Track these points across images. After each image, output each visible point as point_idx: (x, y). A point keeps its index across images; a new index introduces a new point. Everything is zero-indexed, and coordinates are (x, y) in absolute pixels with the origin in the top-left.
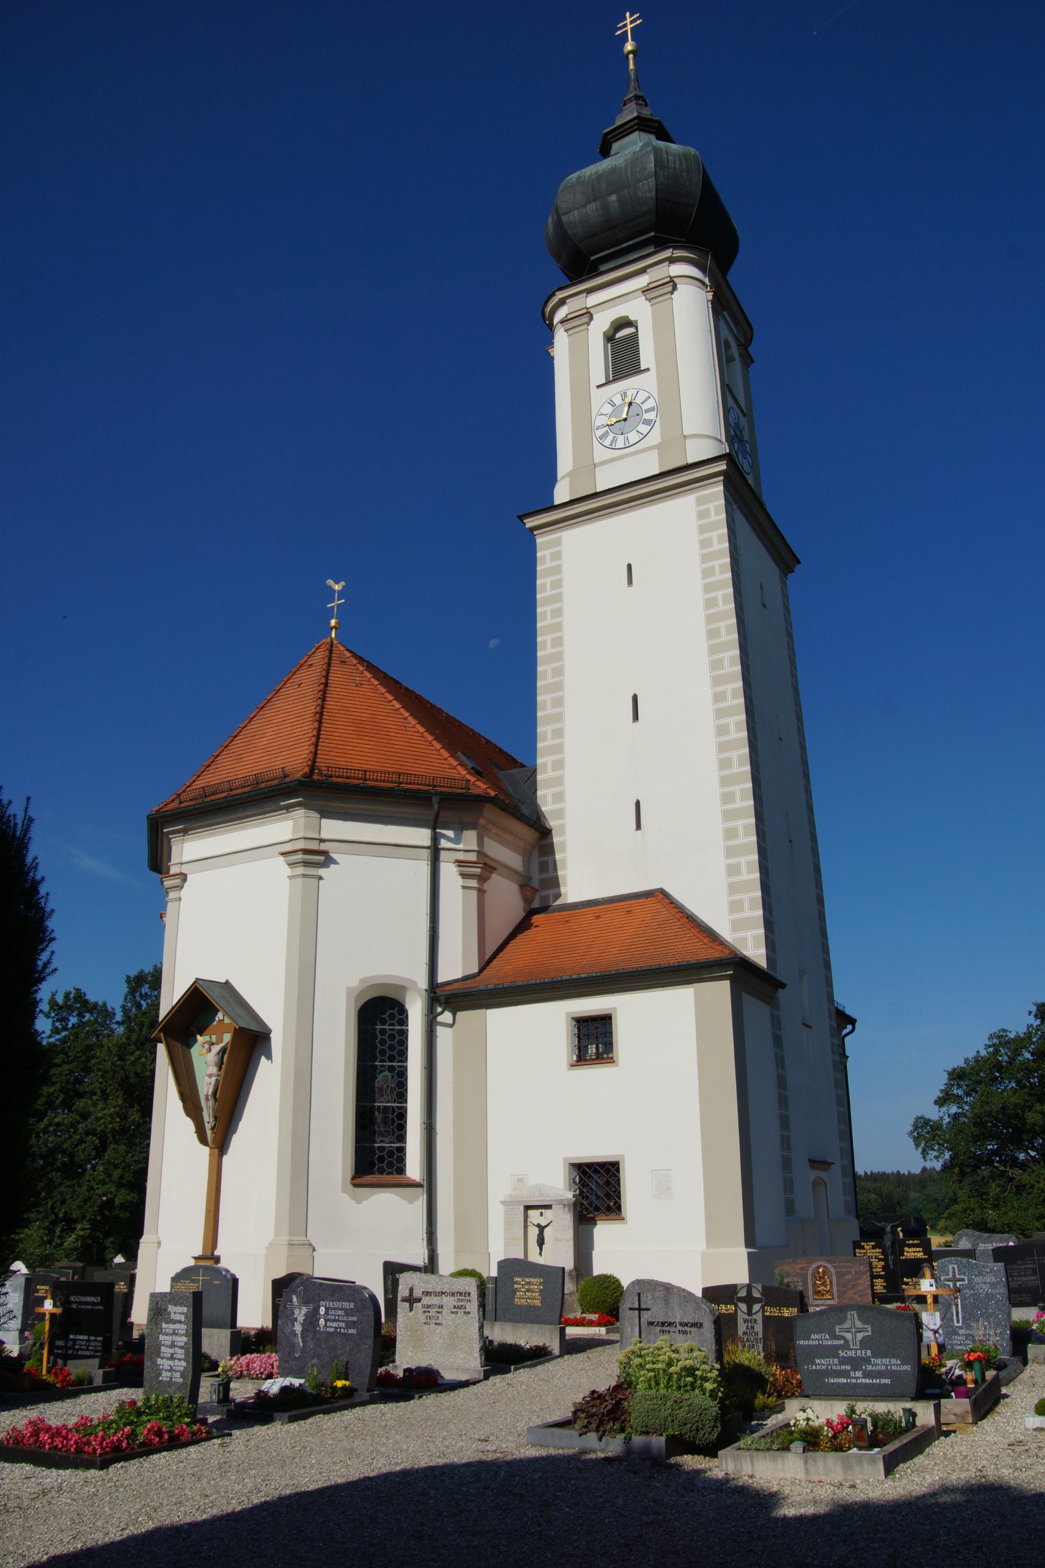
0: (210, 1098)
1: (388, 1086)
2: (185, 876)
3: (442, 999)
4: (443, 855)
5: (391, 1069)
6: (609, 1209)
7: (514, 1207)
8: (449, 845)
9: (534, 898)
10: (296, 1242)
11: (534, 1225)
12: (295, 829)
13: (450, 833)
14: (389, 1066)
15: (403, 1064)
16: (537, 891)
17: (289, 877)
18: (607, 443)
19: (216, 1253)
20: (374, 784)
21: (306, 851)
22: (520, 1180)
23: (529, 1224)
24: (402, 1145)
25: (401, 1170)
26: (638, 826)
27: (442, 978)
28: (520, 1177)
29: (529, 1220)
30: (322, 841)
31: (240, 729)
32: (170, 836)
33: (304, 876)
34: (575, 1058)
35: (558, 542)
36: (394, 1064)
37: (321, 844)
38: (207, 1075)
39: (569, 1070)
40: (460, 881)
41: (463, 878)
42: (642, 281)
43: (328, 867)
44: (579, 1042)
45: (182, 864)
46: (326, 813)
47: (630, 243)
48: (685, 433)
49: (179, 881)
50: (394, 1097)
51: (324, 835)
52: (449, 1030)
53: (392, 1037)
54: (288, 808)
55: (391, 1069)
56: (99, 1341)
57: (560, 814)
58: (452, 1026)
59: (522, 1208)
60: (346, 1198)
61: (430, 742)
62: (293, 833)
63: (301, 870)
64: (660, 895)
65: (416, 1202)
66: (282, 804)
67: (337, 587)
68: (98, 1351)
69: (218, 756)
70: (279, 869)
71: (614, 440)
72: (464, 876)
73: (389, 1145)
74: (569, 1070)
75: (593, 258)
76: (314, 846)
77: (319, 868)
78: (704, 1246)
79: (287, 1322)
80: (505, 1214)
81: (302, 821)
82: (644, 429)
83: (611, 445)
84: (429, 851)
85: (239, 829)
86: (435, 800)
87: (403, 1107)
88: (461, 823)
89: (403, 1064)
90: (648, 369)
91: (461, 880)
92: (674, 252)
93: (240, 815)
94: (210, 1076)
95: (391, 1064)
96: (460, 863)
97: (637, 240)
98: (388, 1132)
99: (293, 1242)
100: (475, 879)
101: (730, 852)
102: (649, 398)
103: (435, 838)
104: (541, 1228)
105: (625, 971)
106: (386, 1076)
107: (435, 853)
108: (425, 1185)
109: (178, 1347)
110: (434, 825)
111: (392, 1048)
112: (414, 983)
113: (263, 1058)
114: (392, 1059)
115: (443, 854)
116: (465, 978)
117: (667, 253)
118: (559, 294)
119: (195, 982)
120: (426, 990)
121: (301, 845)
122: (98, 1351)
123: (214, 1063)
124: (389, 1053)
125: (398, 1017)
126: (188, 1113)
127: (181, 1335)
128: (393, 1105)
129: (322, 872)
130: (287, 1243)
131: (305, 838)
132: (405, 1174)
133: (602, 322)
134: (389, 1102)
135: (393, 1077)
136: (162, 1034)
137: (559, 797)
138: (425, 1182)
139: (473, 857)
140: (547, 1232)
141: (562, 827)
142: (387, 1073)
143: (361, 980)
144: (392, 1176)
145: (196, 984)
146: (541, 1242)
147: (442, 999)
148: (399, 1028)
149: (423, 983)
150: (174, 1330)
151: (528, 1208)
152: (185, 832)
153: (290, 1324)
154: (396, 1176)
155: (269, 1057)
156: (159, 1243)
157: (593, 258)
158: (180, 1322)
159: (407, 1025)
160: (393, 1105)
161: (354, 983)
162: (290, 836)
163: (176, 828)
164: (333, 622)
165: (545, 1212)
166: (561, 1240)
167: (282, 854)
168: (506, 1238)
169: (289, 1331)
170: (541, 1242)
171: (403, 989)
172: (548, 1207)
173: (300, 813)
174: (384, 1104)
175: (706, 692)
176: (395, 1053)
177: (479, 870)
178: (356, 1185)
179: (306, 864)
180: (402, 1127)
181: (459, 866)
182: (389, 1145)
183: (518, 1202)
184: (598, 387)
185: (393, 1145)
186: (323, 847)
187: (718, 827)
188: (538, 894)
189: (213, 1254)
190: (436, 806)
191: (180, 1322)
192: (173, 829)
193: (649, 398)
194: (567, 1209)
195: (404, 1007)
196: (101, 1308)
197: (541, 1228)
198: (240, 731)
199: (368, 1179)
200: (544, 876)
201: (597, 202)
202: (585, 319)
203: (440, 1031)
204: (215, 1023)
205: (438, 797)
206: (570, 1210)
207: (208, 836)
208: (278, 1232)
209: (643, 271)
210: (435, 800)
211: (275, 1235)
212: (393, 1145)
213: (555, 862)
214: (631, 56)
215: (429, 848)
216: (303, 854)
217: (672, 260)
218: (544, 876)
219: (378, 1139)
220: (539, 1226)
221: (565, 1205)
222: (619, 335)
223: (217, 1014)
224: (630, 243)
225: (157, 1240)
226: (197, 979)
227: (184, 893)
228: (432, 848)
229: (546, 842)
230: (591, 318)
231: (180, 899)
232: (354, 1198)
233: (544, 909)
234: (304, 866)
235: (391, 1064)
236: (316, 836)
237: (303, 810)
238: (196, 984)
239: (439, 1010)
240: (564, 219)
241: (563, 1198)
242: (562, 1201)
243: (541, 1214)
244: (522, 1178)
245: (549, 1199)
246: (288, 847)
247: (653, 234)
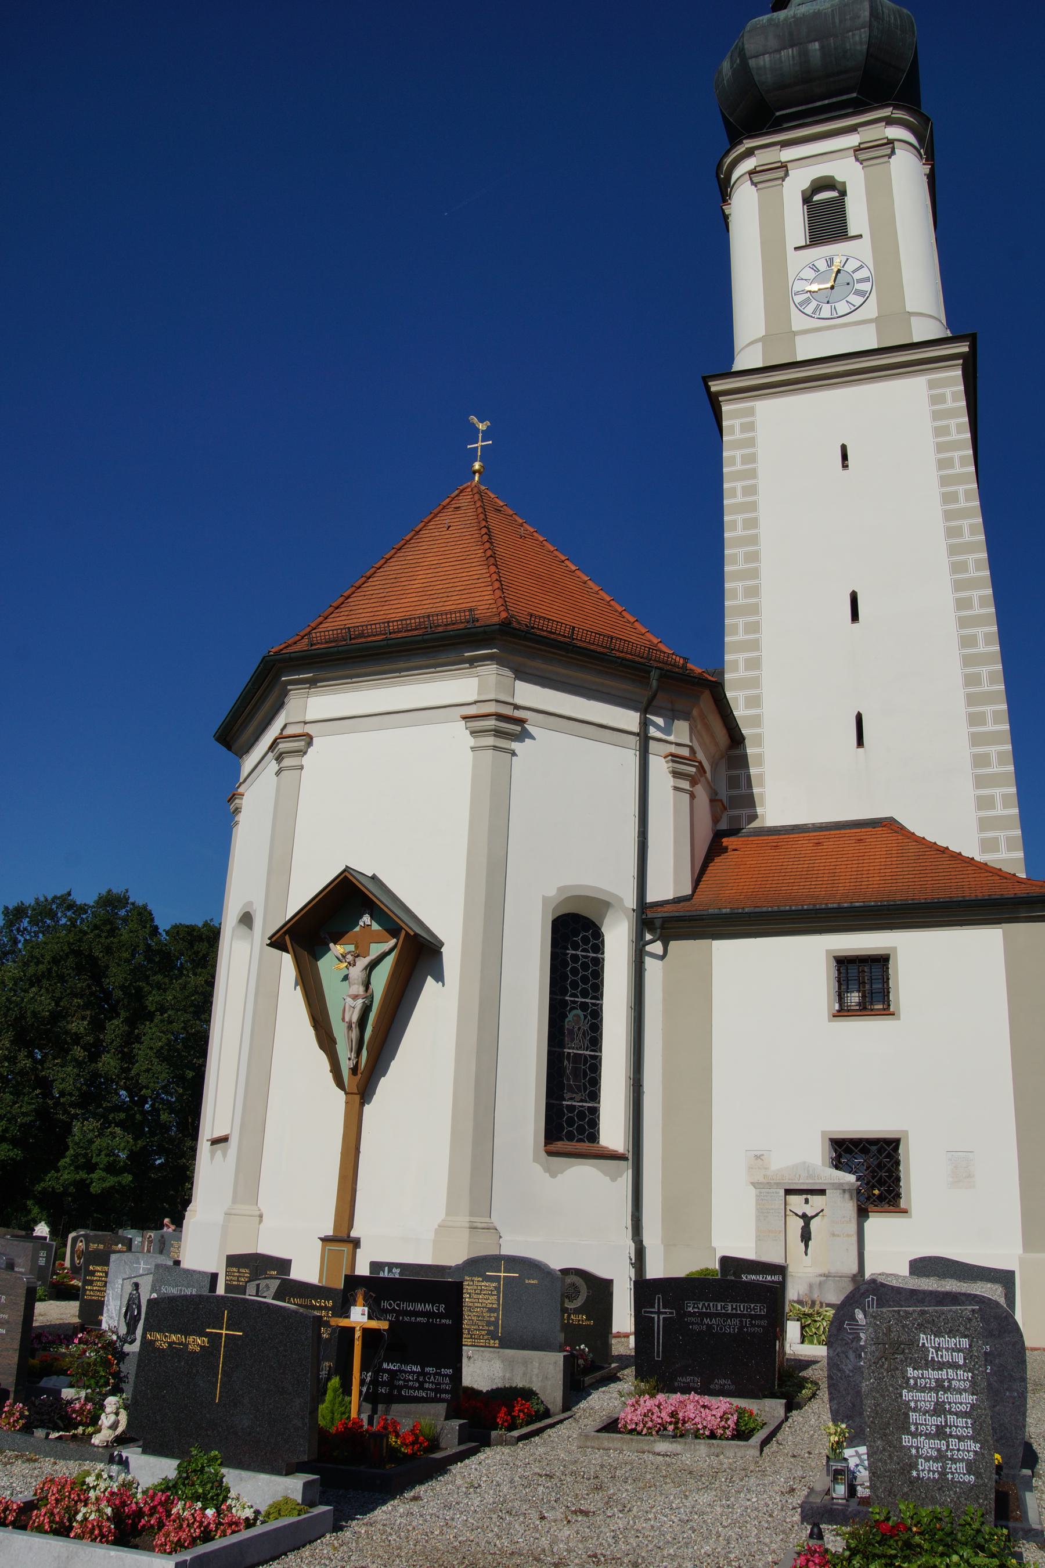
0: (353, 1026)
1: (579, 1029)
2: (311, 738)
3: (658, 923)
4: (653, 745)
5: (584, 1007)
6: (881, 1198)
7: (770, 1191)
8: (658, 734)
9: (721, 817)
10: (479, 1225)
11: (797, 1215)
12: (481, 689)
13: (660, 721)
14: (582, 1002)
15: (598, 1002)
16: (725, 809)
17: (471, 748)
18: (809, 310)
19: (354, 1234)
20: (583, 645)
21: (500, 717)
22: (757, 1157)
23: (788, 1212)
24: (596, 1105)
25: (594, 1137)
26: (860, 742)
27: (651, 898)
28: (758, 1153)
29: (788, 1208)
30: (517, 707)
31: (374, 569)
32: (289, 687)
33: (495, 748)
34: (837, 1007)
35: (751, 412)
36: (587, 1000)
37: (515, 710)
38: (350, 996)
39: (829, 1021)
40: (670, 781)
41: (674, 777)
42: (852, 140)
43: (522, 741)
44: (839, 988)
45: (305, 723)
46: (522, 674)
47: (826, 102)
48: (908, 309)
49: (303, 743)
50: (587, 1042)
51: (518, 701)
52: (659, 963)
53: (584, 966)
54: (472, 662)
55: (584, 1007)
56: (446, 1375)
57: (757, 721)
58: (662, 958)
59: (782, 1192)
60: (538, 1168)
61: (620, 613)
62: (479, 694)
63: (490, 741)
64: (889, 825)
65: (619, 1179)
66: (466, 654)
67: (482, 427)
68: (446, 1391)
69: (349, 597)
70: (459, 735)
71: (818, 309)
72: (676, 774)
73: (580, 1104)
74: (829, 1021)
75: (778, 114)
76: (507, 711)
77: (513, 740)
78: (1021, 1251)
79: (845, 1353)
80: (757, 1200)
81: (492, 679)
82: (857, 300)
83: (814, 312)
84: (638, 738)
85: (394, 685)
86: (654, 674)
87: (597, 1056)
88: (672, 710)
89: (598, 1002)
90: (860, 236)
91: (672, 779)
92: (894, 112)
93: (402, 665)
94: (355, 997)
95: (583, 1000)
96: (674, 758)
97: (834, 100)
98: (578, 1088)
99: (475, 1225)
100: (687, 780)
101: (980, 782)
102: (861, 267)
103: (645, 724)
104: (806, 1219)
105: (916, 902)
106: (578, 1016)
107: (644, 740)
108: (630, 1157)
109: (956, 1414)
110: (646, 709)
111: (585, 980)
112: (621, 900)
113: (430, 980)
114: (585, 994)
115: (652, 744)
116: (677, 900)
117: (886, 112)
118: (747, 143)
119: (344, 871)
120: (634, 910)
121: (491, 708)
122: (446, 1391)
123: (360, 980)
124: (582, 986)
125: (592, 941)
126: (322, 1046)
127: (960, 1392)
128: (586, 1052)
129: (515, 745)
130: (467, 1225)
131: (497, 701)
132: (598, 1142)
133: (800, 180)
134: (580, 1048)
135: (585, 1017)
136: (287, 938)
137: (755, 701)
138: (631, 1153)
139: (685, 752)
140: (814, 1224)
141: (759, 740)
142: (579, 1012)
143: (559, 889)
144: (582, 1144)
145: (346, 874)
146: (806, 1236)
147: (658, 923)
148: (594, 955)
149: (630, 901)
150: (937, 1380)
151: (788, 1192)
152: (313, 683)
153: (851, 1355)
154: (587, 1144)
155: (439, 977)
156: (261, 1216)
157: (778, 114)
158: (954, 1366)
159: (603, 953)
160: (586, 1052)
161: (552, 892)
162: (474, 698)
163: (301, 676)
164: (477, 466)
165: (814, 1199)
166: (838, 1236)
167: (464, 718)
168: (758, 1230)
169: (850, 1367)
170: (806, 1236)
171: (604, 905)
172: (822, 1192)
173: (490, 672)
174: (575, 1051)
175: (947, 597)
176: (588, 986)
177: (694, 769)
178: (550, 1153)
179: (498, 733)
180: (595, 1083)
181: (673, 761)
182: (580, 1104)
183: (778, 1184)
185: (584, 1104)
186: (519, 714)
187: (964, 752)
188: (726, 813)
189: (349, 1236)
190: (654, 683)
191: (954, 1366)
192: (297, 677)
193: (861, 267)
194: (847, 1196)
195: (600, 929)
196: (448, 1322)
197: (806, 1219)
198: (375, 573)
199: (559, 1145)
200: (734, 792)
201: (795, 49)
202: (780, 173)
203: (649, 962)
204: (357, 929)
205: (658, 671)
206: (851, 1198)
208: (451, 1209)
209: (852, 129)
210: (654, 674)
211: (447, 1214)
212: (584, 1104)
213: (749, 777)
215: (638, 735)
216: (496, 720)
218: (734, 792)
219: (567, 1095)
220: (804, 1216)
221: (844, 1191)
222: (816, 198)
223: (361, 917)
224: (826, 102)
225: (258, 1213)
226: (347, 866)
227: (306, 760)
228: (642, 734)
229: (737, 752)
230: (787, 174)
231: (302, 768)
232: (547, 1170)
233: (734, 832)
234: (495, 736)
235: (583, 1000)
236: (510, 700)
237: (495, 666)
238: (346, 874)
239: (648, 937)
240: (752, 63)
241: (841, 1181)
242: (841, 1184)
243: (807, 1201)
244: (763, 1155)
245: (820, 1181)
246: (472, 710)
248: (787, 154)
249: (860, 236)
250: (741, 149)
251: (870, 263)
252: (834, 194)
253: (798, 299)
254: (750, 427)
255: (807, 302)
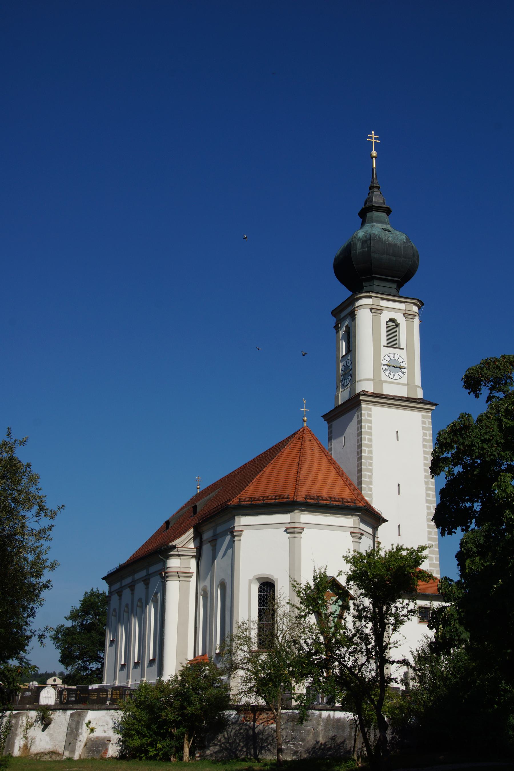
12: (354, 523)
18: (387, 373)
35: (370, 410)
42: (402, 306)
48: (416, 384)
54: (352, 515)
71: (389, 374)
75: (374, 275)
82: (402, 375)
83: (388, 375)
90: (403, 349)
121: (357, 531)
133: (386, 316)
152: (304, 511)
157: (374, 275)
162: (352, 526)
184: (384, 346)
207: (313, 515)
214: (374, 159)
217: (415, 304)
227: (302, 535)
231: (301, 538)
240: (372, 255)
246: (352, 530)
247: (399, 280)
248: (383, 303)
249: (403, 349)
250: (368, 294)
251: (406, 361)
252: (394, 324)
253: (384, 367)
254: (370, 415)
255: (386, 370)
